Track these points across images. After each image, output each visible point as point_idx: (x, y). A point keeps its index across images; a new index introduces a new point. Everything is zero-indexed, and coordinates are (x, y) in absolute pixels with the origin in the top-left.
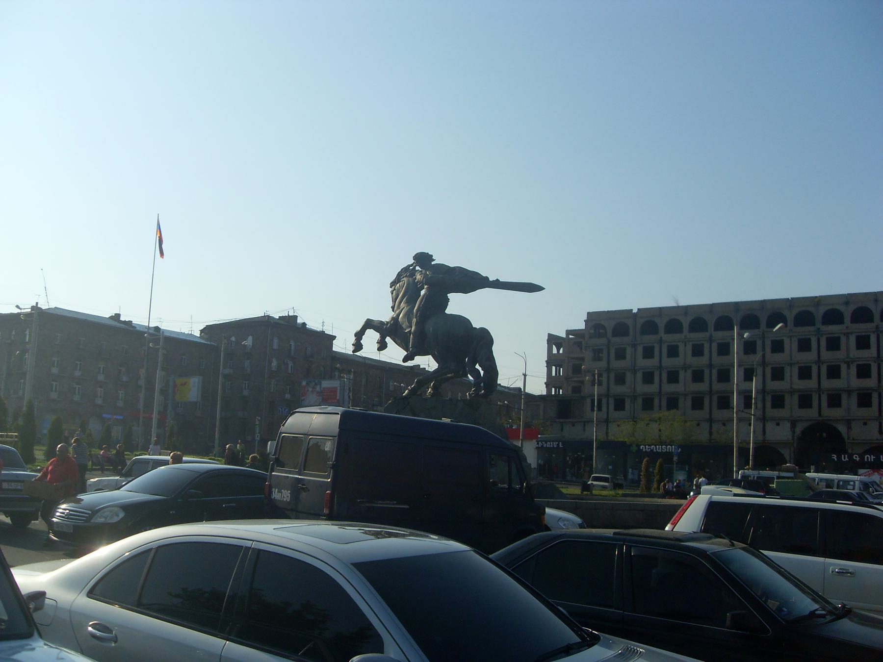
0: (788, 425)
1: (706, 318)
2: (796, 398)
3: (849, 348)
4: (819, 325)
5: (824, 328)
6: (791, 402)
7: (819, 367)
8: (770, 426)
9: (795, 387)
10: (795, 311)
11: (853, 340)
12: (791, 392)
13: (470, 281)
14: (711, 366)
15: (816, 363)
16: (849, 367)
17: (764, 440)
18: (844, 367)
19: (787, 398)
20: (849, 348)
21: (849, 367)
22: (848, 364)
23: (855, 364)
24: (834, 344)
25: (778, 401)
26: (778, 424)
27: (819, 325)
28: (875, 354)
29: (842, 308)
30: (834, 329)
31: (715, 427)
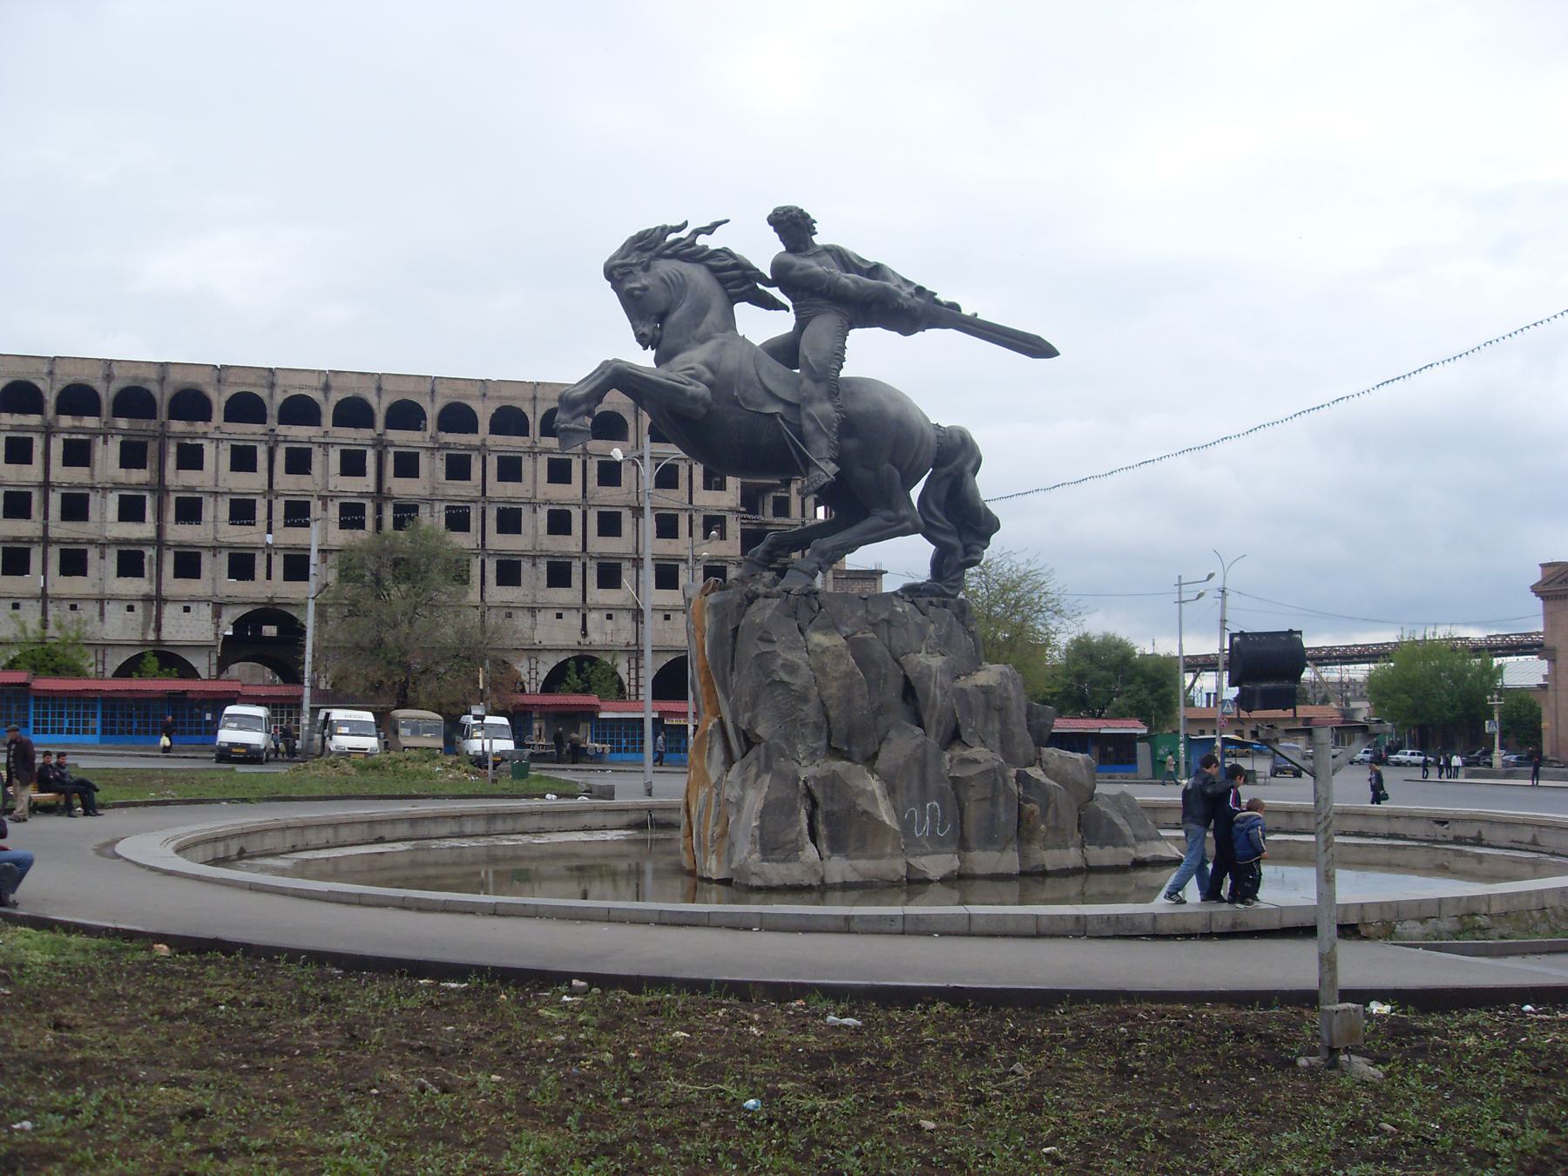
0: (206, 611)
1: (40, 384)
2: (224, 558)
3: (327, 472)
4: (272, 422)
5: (283, 430)
6: (214, 568)
7: (270, 503)
8: (171, 612)
9: (221, 537)
10: (229, 392)
11: (335, 457)
12: (215, 549)
13: (911, 311)
14: (46, 486)
15: (263, 494)
16: (325, 505)
17: (158, 640)
18: (316, 508)
19: (206, 559)
20: (327, 472)
21: (325, 505)
22: (323, 499)
23: (337, 502)
24: (299, 462)
25: (188, 565)
26: (187, 609)
27: (272, 422)
28: (372, 489)
29: (317, 396)
30: (300, 433)
31: (53, 611)
